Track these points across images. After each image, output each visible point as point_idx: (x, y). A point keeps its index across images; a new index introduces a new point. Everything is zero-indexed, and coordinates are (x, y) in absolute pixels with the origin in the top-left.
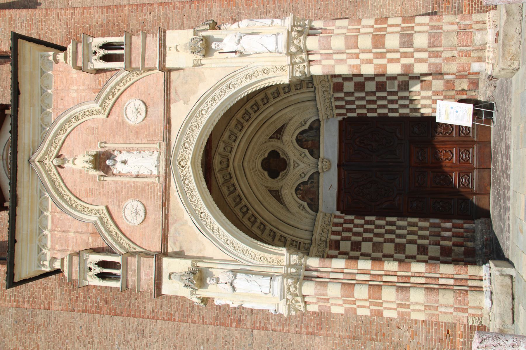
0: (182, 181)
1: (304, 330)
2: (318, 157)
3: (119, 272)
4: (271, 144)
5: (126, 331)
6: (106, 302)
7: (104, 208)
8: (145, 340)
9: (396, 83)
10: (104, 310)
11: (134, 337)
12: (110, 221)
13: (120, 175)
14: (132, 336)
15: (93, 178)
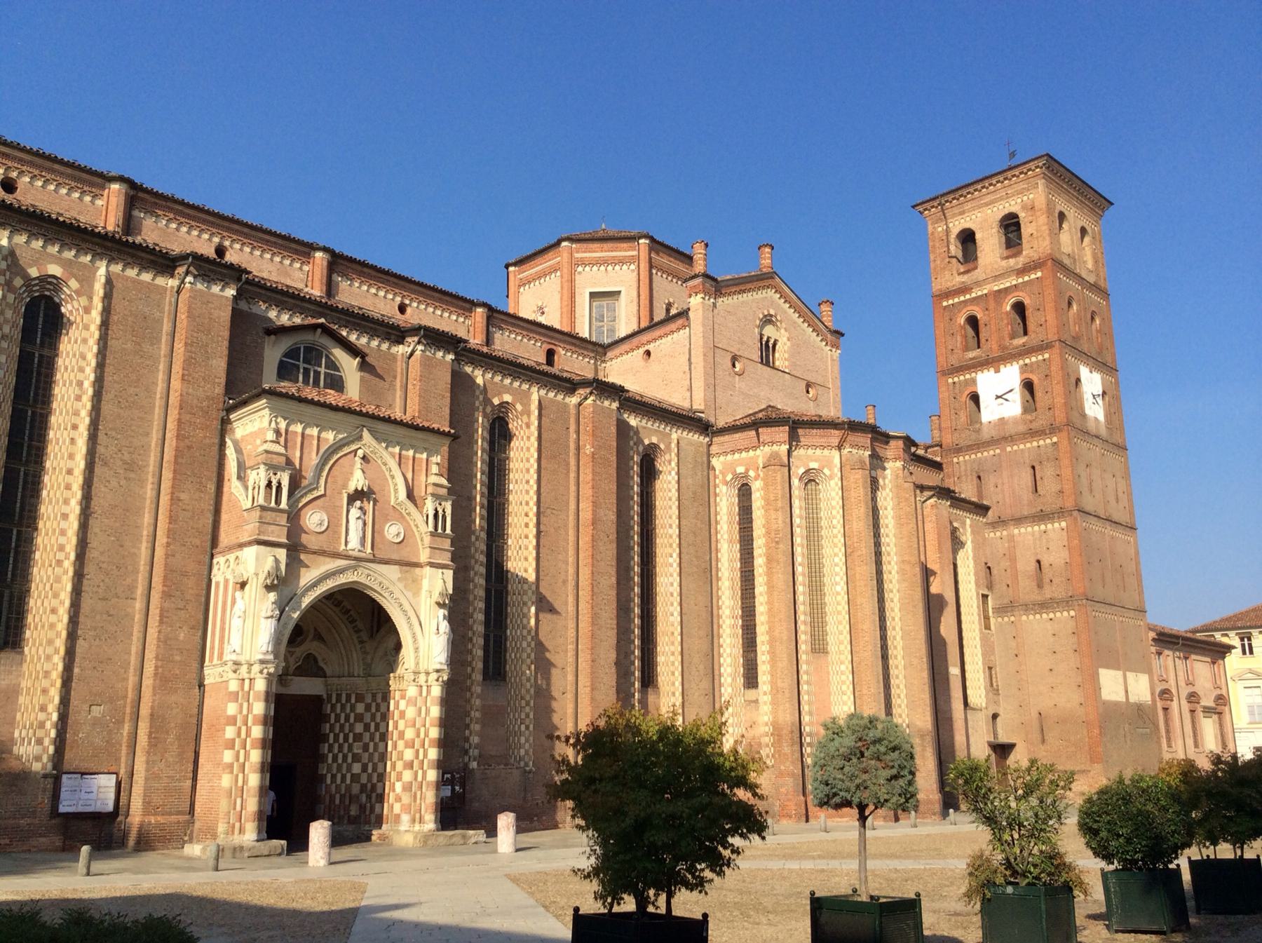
0: (341, 571)
1: (160, 663)
2: (294, 675)
3: (273, 504)
4: (312, 631)
5: (132, 449)
6: (189, 448)
7: (322, 492)
8: (122, 472)
9: (360, 751)
10: (182, 444)
11: (125, 458)
12: (312, 497)
13: (348, 511)
14: (127, 457)
15: (345, 486)
